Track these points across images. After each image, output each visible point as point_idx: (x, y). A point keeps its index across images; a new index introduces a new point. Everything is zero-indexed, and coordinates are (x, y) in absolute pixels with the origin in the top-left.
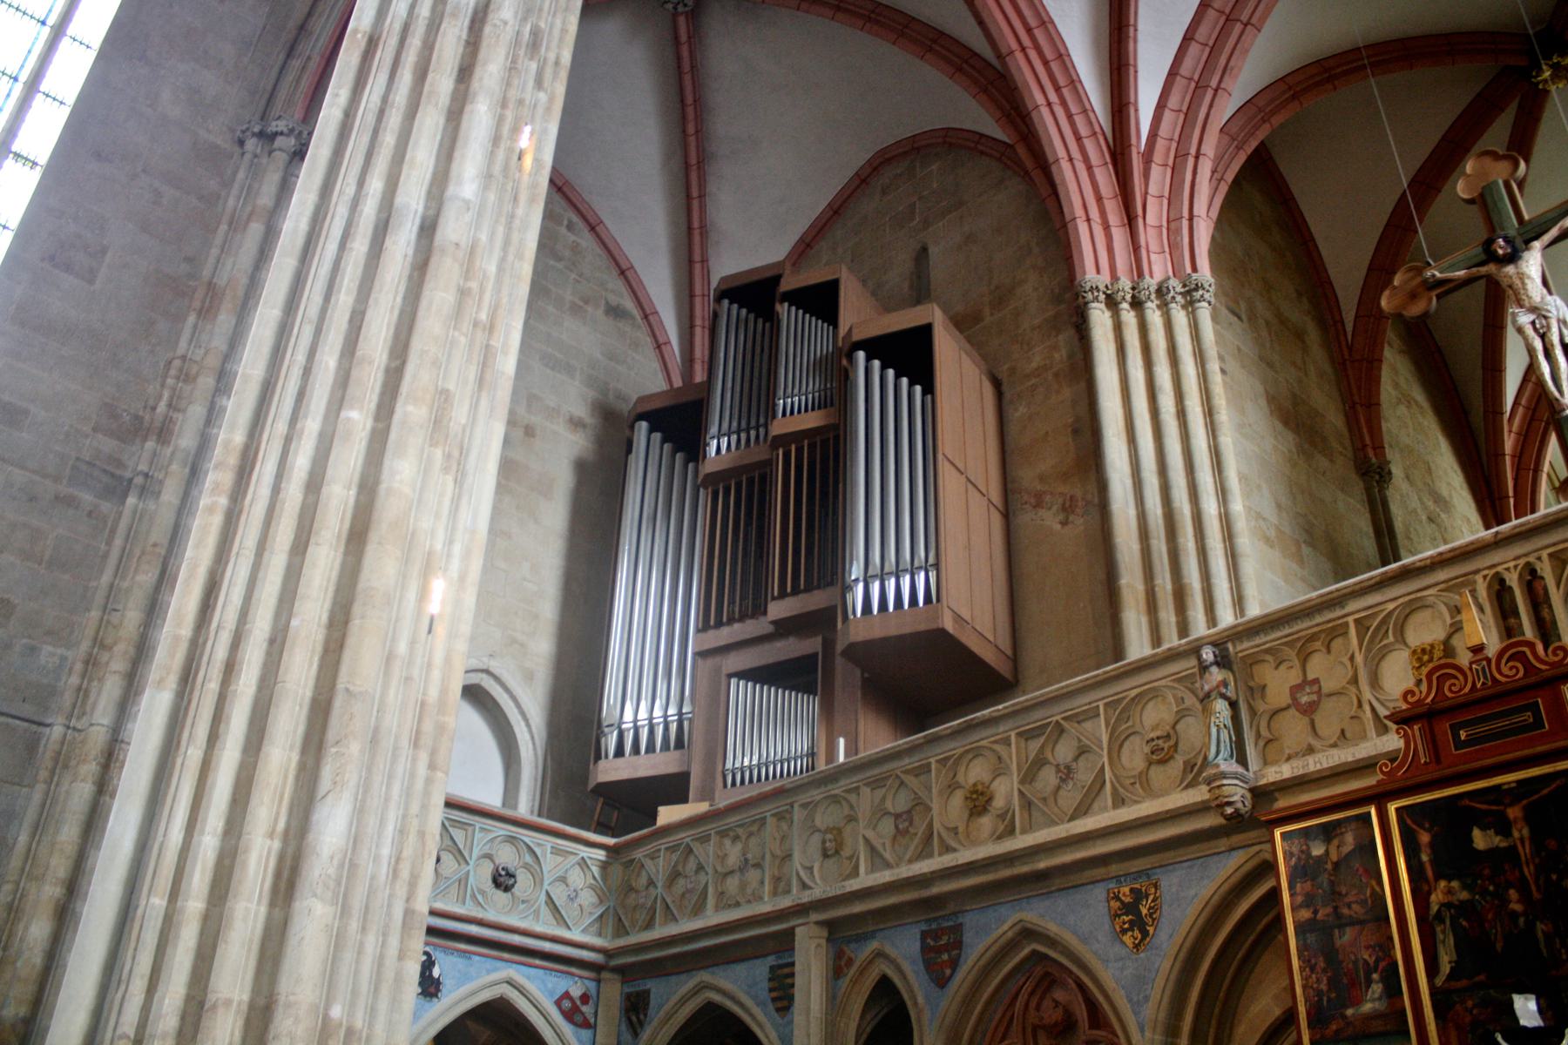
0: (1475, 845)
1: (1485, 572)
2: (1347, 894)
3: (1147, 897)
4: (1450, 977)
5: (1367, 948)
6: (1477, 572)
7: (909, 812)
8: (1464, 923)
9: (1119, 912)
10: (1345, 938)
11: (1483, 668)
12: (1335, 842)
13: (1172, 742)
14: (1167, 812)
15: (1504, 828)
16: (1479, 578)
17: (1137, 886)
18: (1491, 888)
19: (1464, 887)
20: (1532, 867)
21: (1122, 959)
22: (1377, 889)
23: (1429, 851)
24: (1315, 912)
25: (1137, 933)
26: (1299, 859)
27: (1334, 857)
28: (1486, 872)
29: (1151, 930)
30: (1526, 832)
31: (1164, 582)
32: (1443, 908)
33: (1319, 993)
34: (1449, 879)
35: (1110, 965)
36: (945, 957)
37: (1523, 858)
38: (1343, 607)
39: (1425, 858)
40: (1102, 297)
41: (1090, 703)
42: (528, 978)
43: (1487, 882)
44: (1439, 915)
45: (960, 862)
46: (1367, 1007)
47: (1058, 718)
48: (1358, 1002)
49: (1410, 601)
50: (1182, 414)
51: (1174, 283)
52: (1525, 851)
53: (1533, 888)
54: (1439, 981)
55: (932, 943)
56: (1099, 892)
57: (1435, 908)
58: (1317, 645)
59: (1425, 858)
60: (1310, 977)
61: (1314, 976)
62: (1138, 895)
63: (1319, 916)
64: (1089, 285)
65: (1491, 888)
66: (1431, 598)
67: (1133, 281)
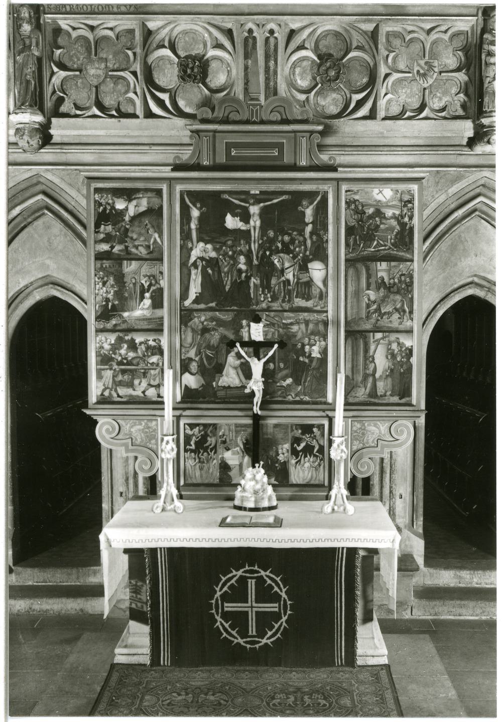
0: (226, 225)
2: (135, 240)
4: (197, 301)
5: (145, 276)
8: (210, 271)
10: (130, 268)
11: (257, 110)
12: (134, 202)
15: (245, 217)
18: (230, 253)
19: (215, 249)
20: (257, 245)
22: (158, 240)
23: (196, 222)
26: (105, 209)
27: (131, 212)
28: (229, 243)
30: (258, 223)
32: (198, 260)
37: (253, 239)
39: (193, 226)
43: (229, 249)
44: (195, 265)
46: (138, 313)
53: (255, 257)
57: (193, 259)
59: (193, 226)
60: (102, 288)
61: (104, 289)
63: (116, 250)
65: (230, 253)
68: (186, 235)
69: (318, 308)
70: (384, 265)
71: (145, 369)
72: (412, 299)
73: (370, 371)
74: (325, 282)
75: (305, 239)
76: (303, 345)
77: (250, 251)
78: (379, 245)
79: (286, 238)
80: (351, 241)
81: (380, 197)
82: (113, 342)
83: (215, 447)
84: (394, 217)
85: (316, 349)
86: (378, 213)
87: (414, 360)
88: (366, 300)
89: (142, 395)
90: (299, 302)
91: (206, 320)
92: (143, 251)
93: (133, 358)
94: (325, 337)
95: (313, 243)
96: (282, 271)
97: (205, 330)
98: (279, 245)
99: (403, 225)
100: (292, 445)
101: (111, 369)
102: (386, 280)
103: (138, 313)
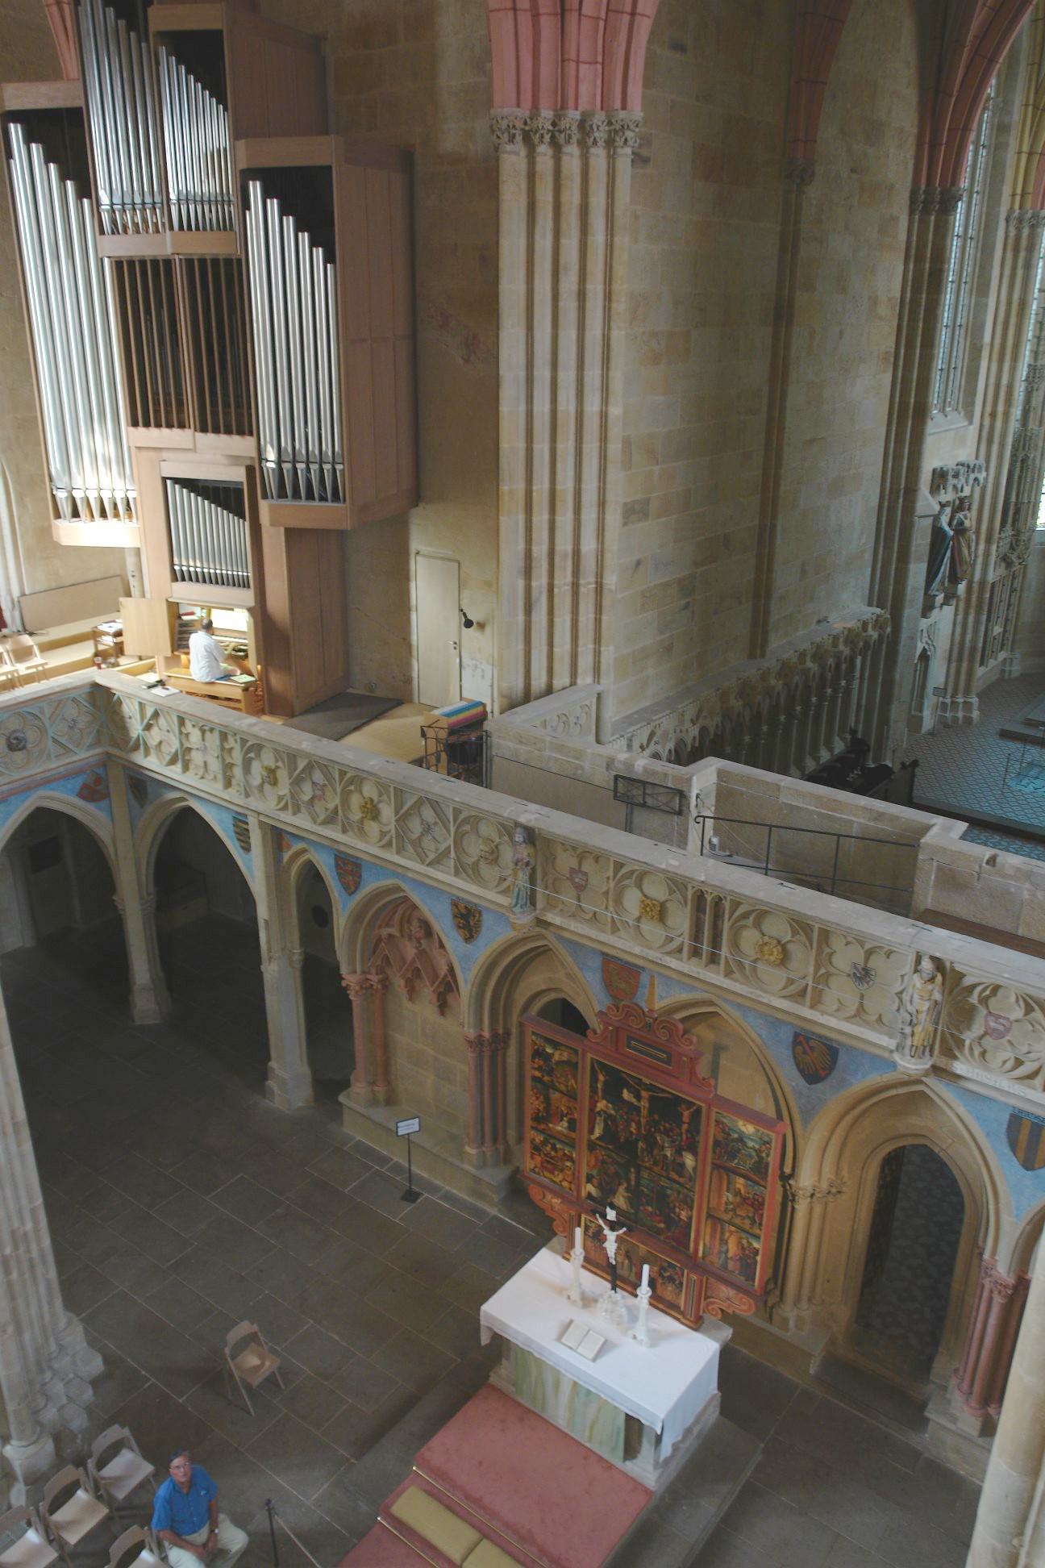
4: (598, 1139)
13: (495, 856)
15: (638, 1097)
27: (557, 1057)
30: (647, 1105)
31: (541, 486)
34: (608, 1102)
40: (519, 138)
42: (53, 790)
44: (599, 1113)
46: (559, 1128)
50: (582, 295)
51: (599, 118)
52: (644, 1112)
54: (593, 1137)
57: (598, 1109)
59: (600, 1085)
64: (505, 122)
67: (555, 110)
68: (594, 1090)
70: (741, 1180)
72: (762, 1215)
73: (724, 1249)
74: (695, 1169)
75: (681, 1133)
76: (675, 1207)
77: (639, 1121)
78: (738, 1164)
79: (667, 1125)
80: (718, 1151)
81: (743, 1129)
84: (753, 1148)
86: (741, 1140)
87: (759, 1258)
88: (725, 1199)
90: (673, 1175)
92: (563, 1088)
94: (691, 1209)
95: (687, 1138)
96: (663, 1148)
97: (603, 1162)
98: (662, 1128)
99: (761, 1158)
100: (660, 1270)
102: (743, 1191)
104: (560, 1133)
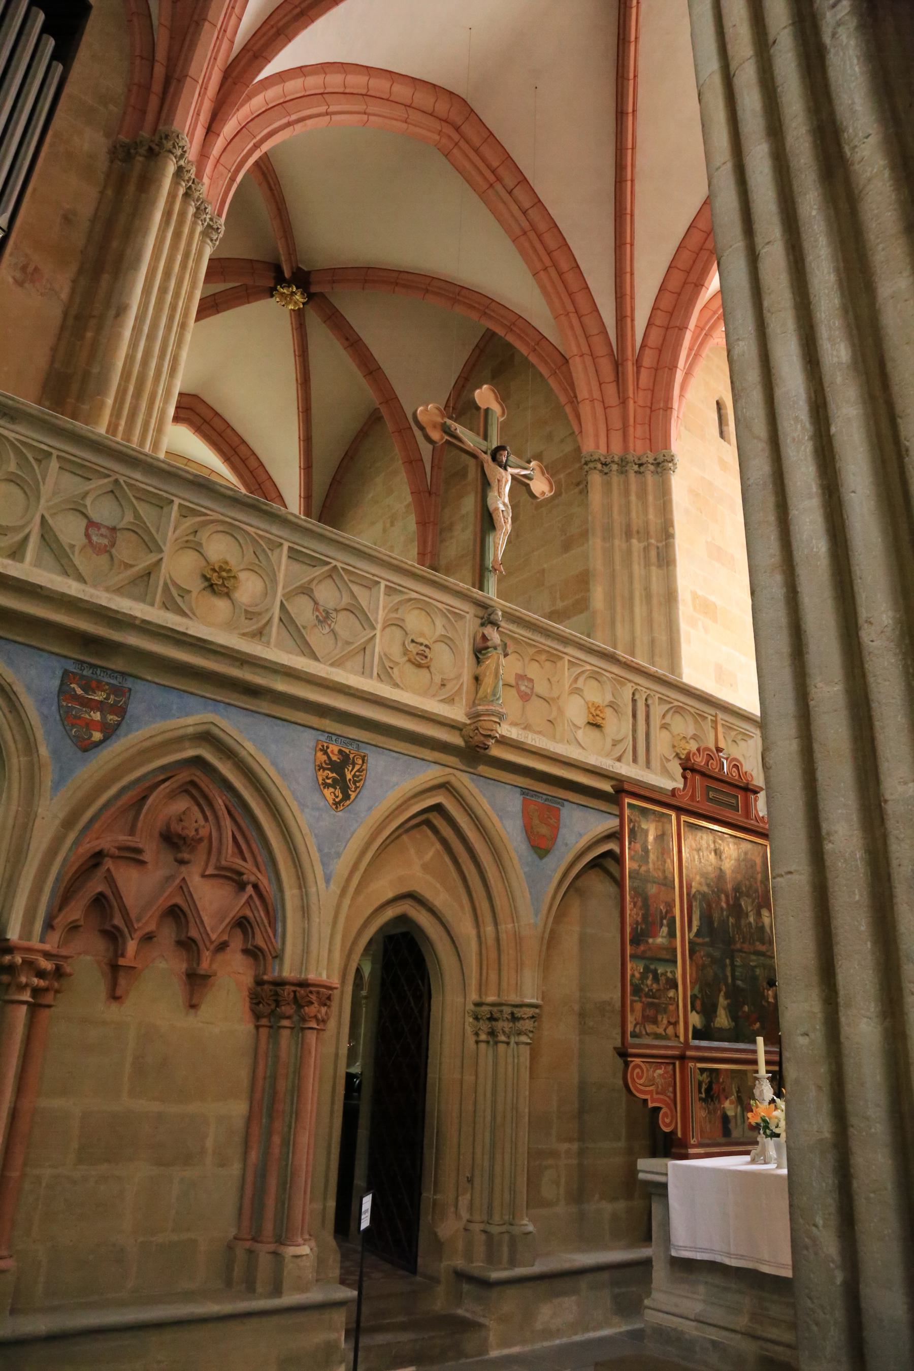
1: (633, 685)
3: (354, 764)
4: (698, 934)
6: (630, 681)
7: (114, 529)
9: (324, 765)
14: (423, 711)
16: (630, 685)
17: (347, 751)
21: (318, 809)
24: (640, 866)
25: (338, 792)
29: (352, 797)
33: (637, 923)
35: (307, 810)
36: (97, 716)
38: (565, 647)
41: (374, 575)
44: (694, 895)
45: (190, 632)
47: (339, 565)
48: (655, 936)
49: (598, 673)
55: (79, 691)
56: (308, 739)
58: (543, 657)
62: (346, 759)
66: (605, 678)
69: (769, 953)
71: (666, 1004)
76: (764, 990)
82: (642, 970)
83: (718, 1095)
85: (770, 992)
89: (664, 1033)
91: (704, 956)
93: (658, 990)
101: (641, 1001)
103: (659, 940)
104: (661, 948)
